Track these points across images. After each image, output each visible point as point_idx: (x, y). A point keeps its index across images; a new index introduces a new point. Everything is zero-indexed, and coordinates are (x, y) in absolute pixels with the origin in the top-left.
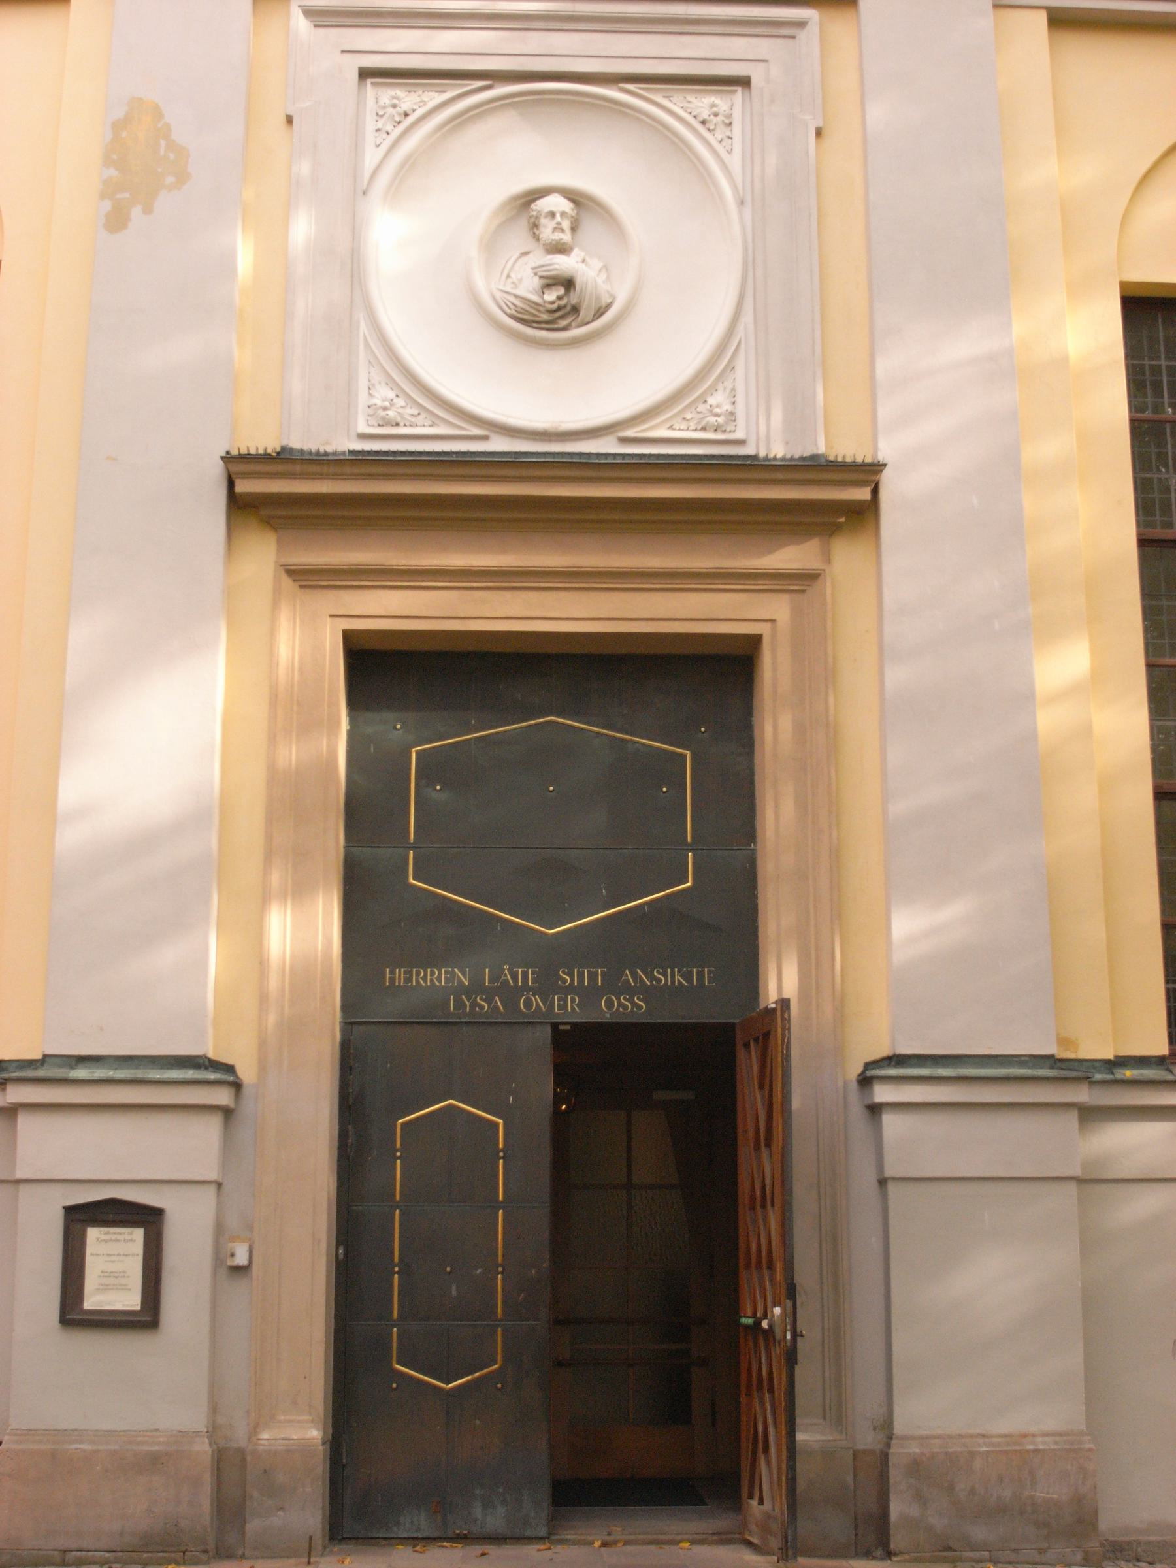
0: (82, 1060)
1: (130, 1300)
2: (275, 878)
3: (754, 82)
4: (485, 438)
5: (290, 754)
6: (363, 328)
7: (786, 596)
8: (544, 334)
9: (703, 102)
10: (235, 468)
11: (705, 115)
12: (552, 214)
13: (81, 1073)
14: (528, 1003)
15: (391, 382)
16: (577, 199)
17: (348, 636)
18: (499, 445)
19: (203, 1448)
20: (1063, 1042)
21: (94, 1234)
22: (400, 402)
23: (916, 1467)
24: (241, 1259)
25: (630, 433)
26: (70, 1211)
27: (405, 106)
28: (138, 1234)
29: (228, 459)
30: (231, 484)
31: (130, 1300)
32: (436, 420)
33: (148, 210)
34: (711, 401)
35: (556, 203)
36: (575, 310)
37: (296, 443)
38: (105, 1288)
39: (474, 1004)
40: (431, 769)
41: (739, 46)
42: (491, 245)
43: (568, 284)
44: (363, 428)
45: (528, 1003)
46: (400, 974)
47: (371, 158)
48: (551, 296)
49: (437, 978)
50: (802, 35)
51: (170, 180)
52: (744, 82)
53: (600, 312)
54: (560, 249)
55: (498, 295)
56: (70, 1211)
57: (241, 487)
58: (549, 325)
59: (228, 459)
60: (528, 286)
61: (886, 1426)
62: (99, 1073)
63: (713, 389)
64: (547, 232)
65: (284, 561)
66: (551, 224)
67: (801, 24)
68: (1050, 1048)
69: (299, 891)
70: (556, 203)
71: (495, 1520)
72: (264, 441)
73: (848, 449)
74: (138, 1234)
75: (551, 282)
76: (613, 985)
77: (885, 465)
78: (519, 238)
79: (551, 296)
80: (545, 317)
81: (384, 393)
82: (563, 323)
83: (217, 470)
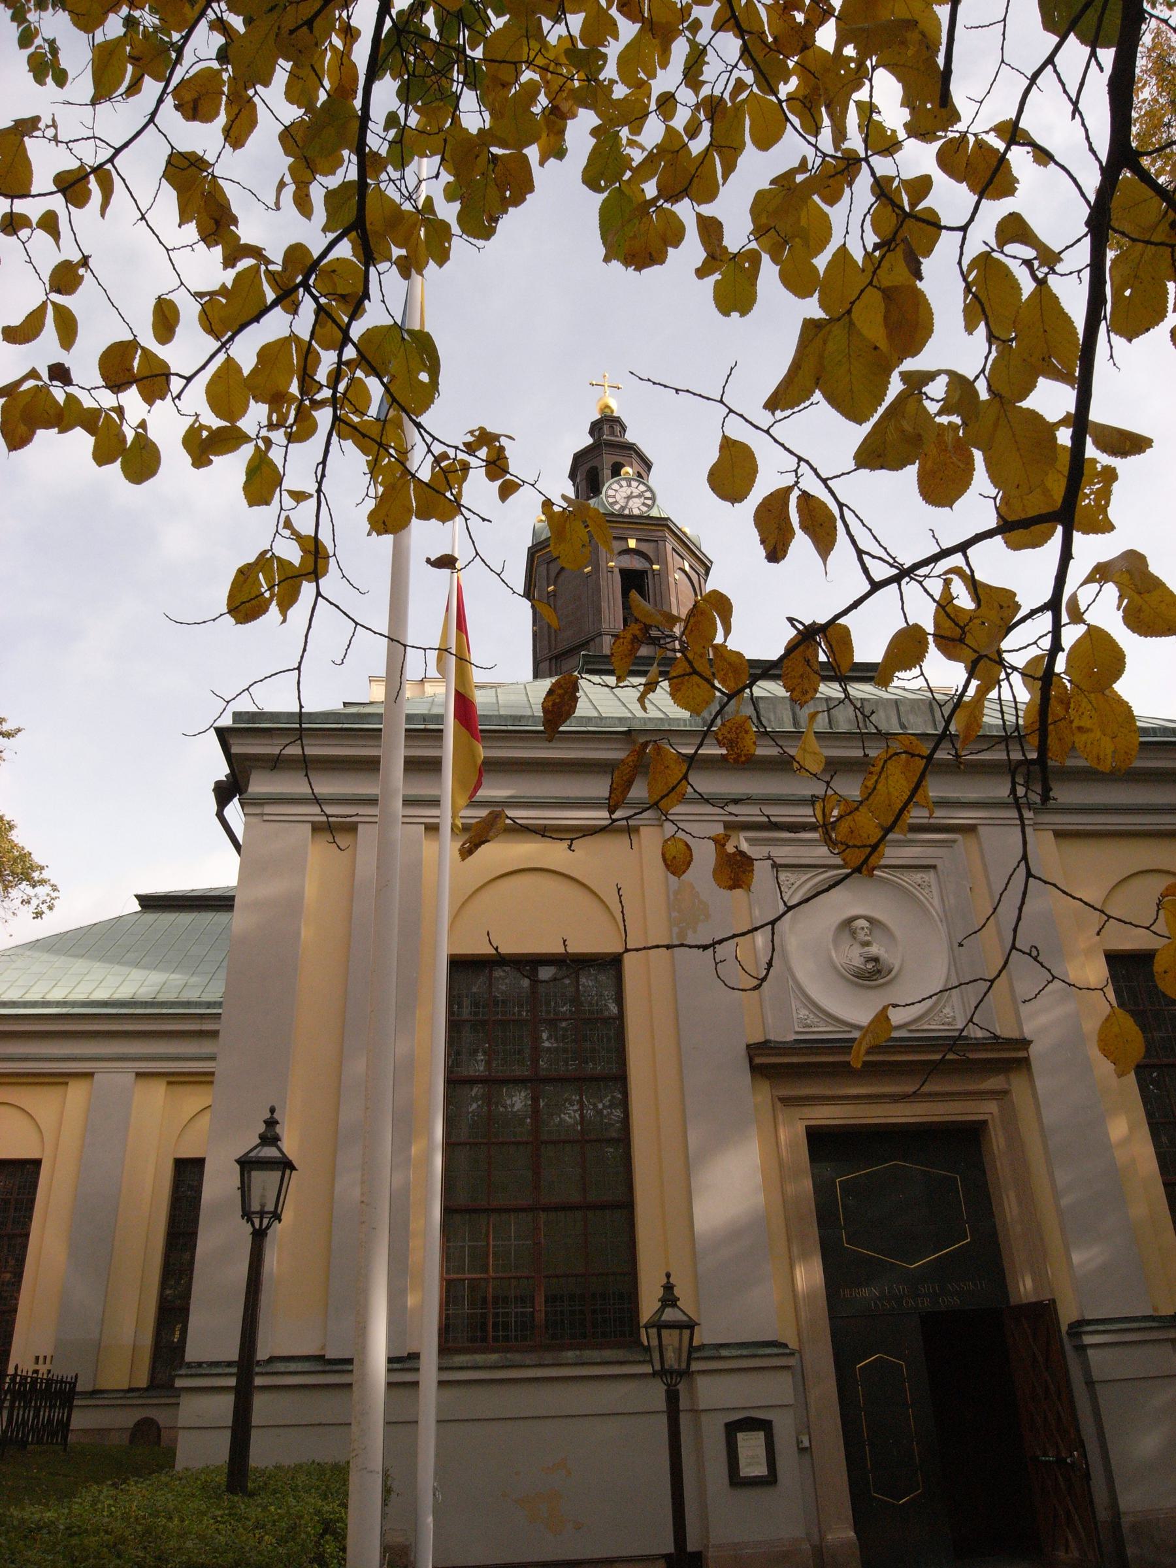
0: (722, 1346)
1: (761, 1470)
2: (795, 1250)
3: (938, 867)
4: (849, 1032)
5: (790, 1189)
6: (791, 983)
7: (995, 1102)
8: (861, 981)
9: (918, 877)
10: (752, 1053)
11: (920, 882)
12: (863, 928)
13: (724, 1353)
14: (907, 1303)
15: (806, 1007)
17: (807, 1127)
19: (806, 1546)
20: (1155, 1309)
21: (740, 1436)
22: (812, 1016)
24: (806, 1444)
25: (913, 1027)
26: (727, 1425)
27: (792, 881)
28: (761, 1434)
29: (748, 1046)
30: (751, 1060)
31: (761, 1470)
32: (828, 1024)
33: (695, 932)
34: (944, 1011)
35: (862, 923)
36: (879, 971)
37: (772, 1037)
38: (749, 1464)
39: (883, 1305)
40: (846, 1188)
41: (930, 851)
42: (836, 941)
43: (876, 960)
44: (798, 1029)
45: (907, 1303)
46: (847, 1292)
48: (870, 966)
49: (864, 1293)
50: (955, 846)
51: (702, 917)
52: (934, 867)
53: (890, 971)
54: (867, 944)
55: (844, 965)
56: (727, 1425)
57: (758, 1060)
58: (868, 979)
59: (748, 1046)
60: (858, 962)
62: (735, 1352)
63: (944, 1006)
64: (861, 936)
65: (777, 1094)
66: (863, 933)
67: (954, 841)
68: (1150, 1312)
69: (805, 1256)
70: (862, 923)
72: (758, 1038)
74: (761, 1434)
77: (1032, 1042)
78: (846, 936)
79: (870, 966)
80: (867, 975)
81: (803, 1013)
82: (875, 977)
83: (743, 1052)
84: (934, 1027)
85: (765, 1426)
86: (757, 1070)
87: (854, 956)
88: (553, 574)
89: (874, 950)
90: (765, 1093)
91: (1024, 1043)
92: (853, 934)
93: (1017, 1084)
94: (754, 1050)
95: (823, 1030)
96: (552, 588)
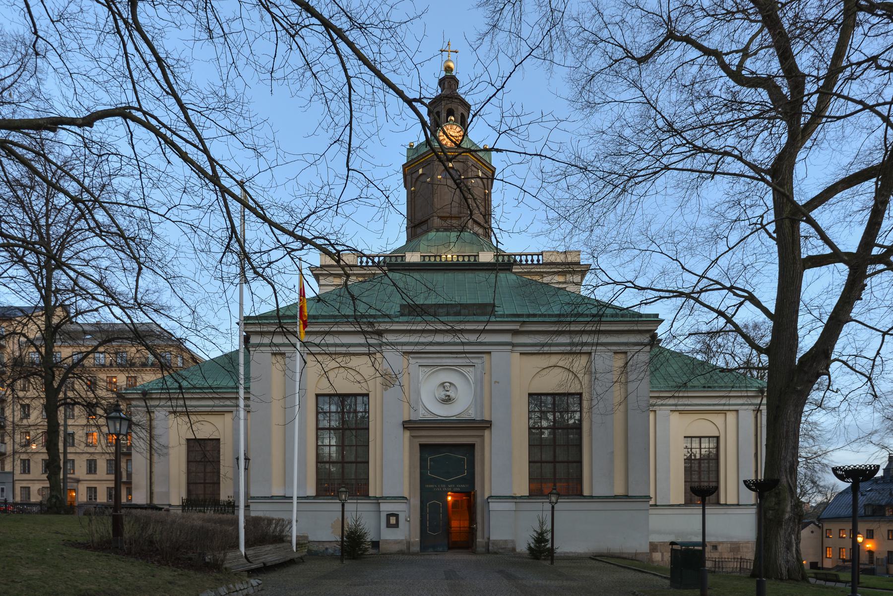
9: (468, 369)
16: (450, 383)
18: (439, 418)
23: (493, 543)
41: (473, 361)
47: (421, 378)
54: (448, 391)
56: (387, 515)
60: (444, 397)
61: (489, 539)
71: (441, 550)
73: (487, 419)
75: (447, 396)
76: (456, 487)
78: (442, 389)
81: (424, 412)
84: (466, 417)
85: (397, 516)
86: (404, 428)
87: (442, 394)
88: (414, 180)
89: (448, 393)
90: (407, 434)
91: (490, 422)
92: (444, 387)
93: (487, 433)
94: (404, 422)
95: (429, 417)
96: (413, 189)
